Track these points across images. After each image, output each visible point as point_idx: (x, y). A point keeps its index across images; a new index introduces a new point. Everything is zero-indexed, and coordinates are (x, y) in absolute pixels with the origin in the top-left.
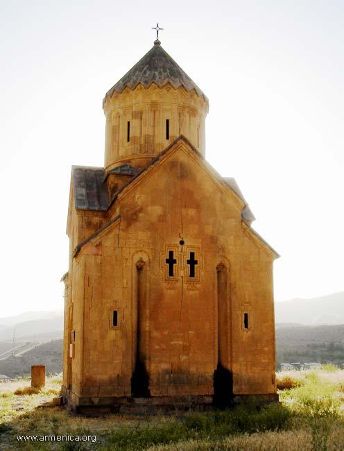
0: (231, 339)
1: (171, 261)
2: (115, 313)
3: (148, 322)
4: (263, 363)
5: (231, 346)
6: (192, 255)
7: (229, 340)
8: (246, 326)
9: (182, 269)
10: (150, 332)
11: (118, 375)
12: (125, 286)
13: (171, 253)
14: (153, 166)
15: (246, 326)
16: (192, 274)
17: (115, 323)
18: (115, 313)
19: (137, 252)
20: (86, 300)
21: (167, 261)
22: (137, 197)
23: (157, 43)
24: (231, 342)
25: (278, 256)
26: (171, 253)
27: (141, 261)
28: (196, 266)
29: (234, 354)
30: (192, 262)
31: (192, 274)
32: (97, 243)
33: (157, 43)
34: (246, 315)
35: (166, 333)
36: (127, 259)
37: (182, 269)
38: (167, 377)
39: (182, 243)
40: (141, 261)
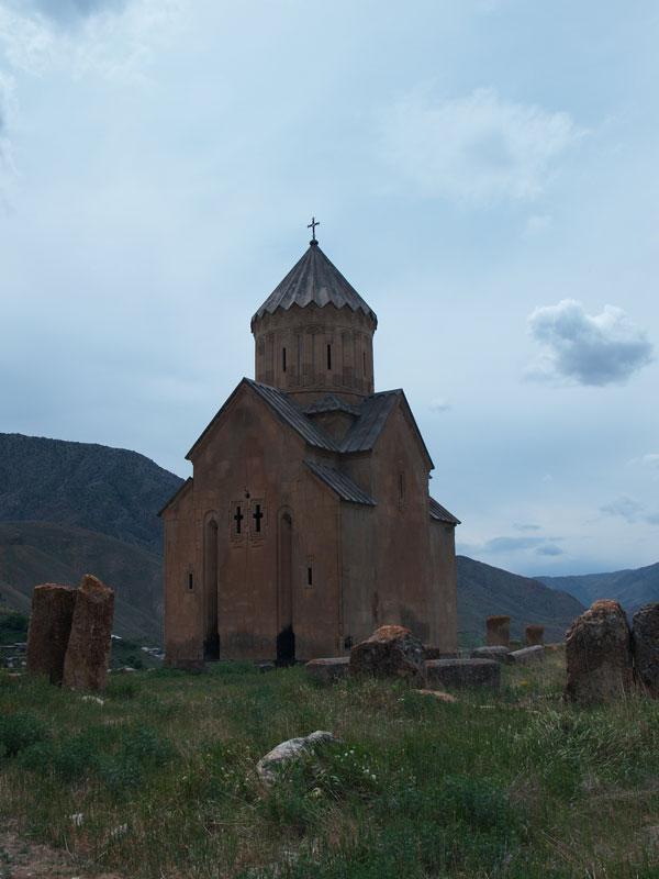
1: (239, 517)
6: (258, 507)
8: (310, 583)
9: (248, 522)
19: (209, 512)
23: (314, 243)
27: (213, 521)
30: (258, 516)
33: (314, 243)
34: (310, 570)
37: (248, 522)
39: (248, 496)
40: (213, 521)
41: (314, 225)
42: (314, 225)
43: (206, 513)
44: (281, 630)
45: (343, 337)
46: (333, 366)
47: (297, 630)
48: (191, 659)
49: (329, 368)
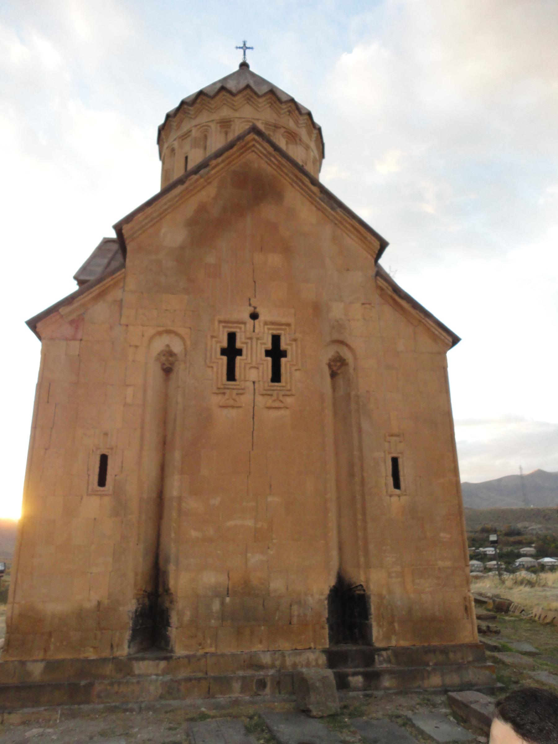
0: (364, 514)
2: (104, 459)
3: (177, 477)
4: (439, 569)
5: (365, 529)
6: (276, 339)
7: (360, 516)
8: (397, 485)
10: (180, 499)
11: (99, 603)
12: (129, 400)
13: (232, 337)
15: (397, 485)
16: (276, 377)
17: (102, 482)
18: (104, 459)
21: (224, 352)
22: (163, 231)
23: (244, 65)
24: (364, 521)
25: (455, 340)
26: (232, 337)
27: (169, 353)
28: (283, 360)
29: (371, 546)
31: (276, 377)
32: (74, 316)
33: (244, 65)
34: (395, 461)
35: (216, 501)
36: (136, 347)
38: (216, 606)
39: (254, 316)
40: (169, 353)
42: (245, 48)
44: (332, 582)
48: (91, 655)
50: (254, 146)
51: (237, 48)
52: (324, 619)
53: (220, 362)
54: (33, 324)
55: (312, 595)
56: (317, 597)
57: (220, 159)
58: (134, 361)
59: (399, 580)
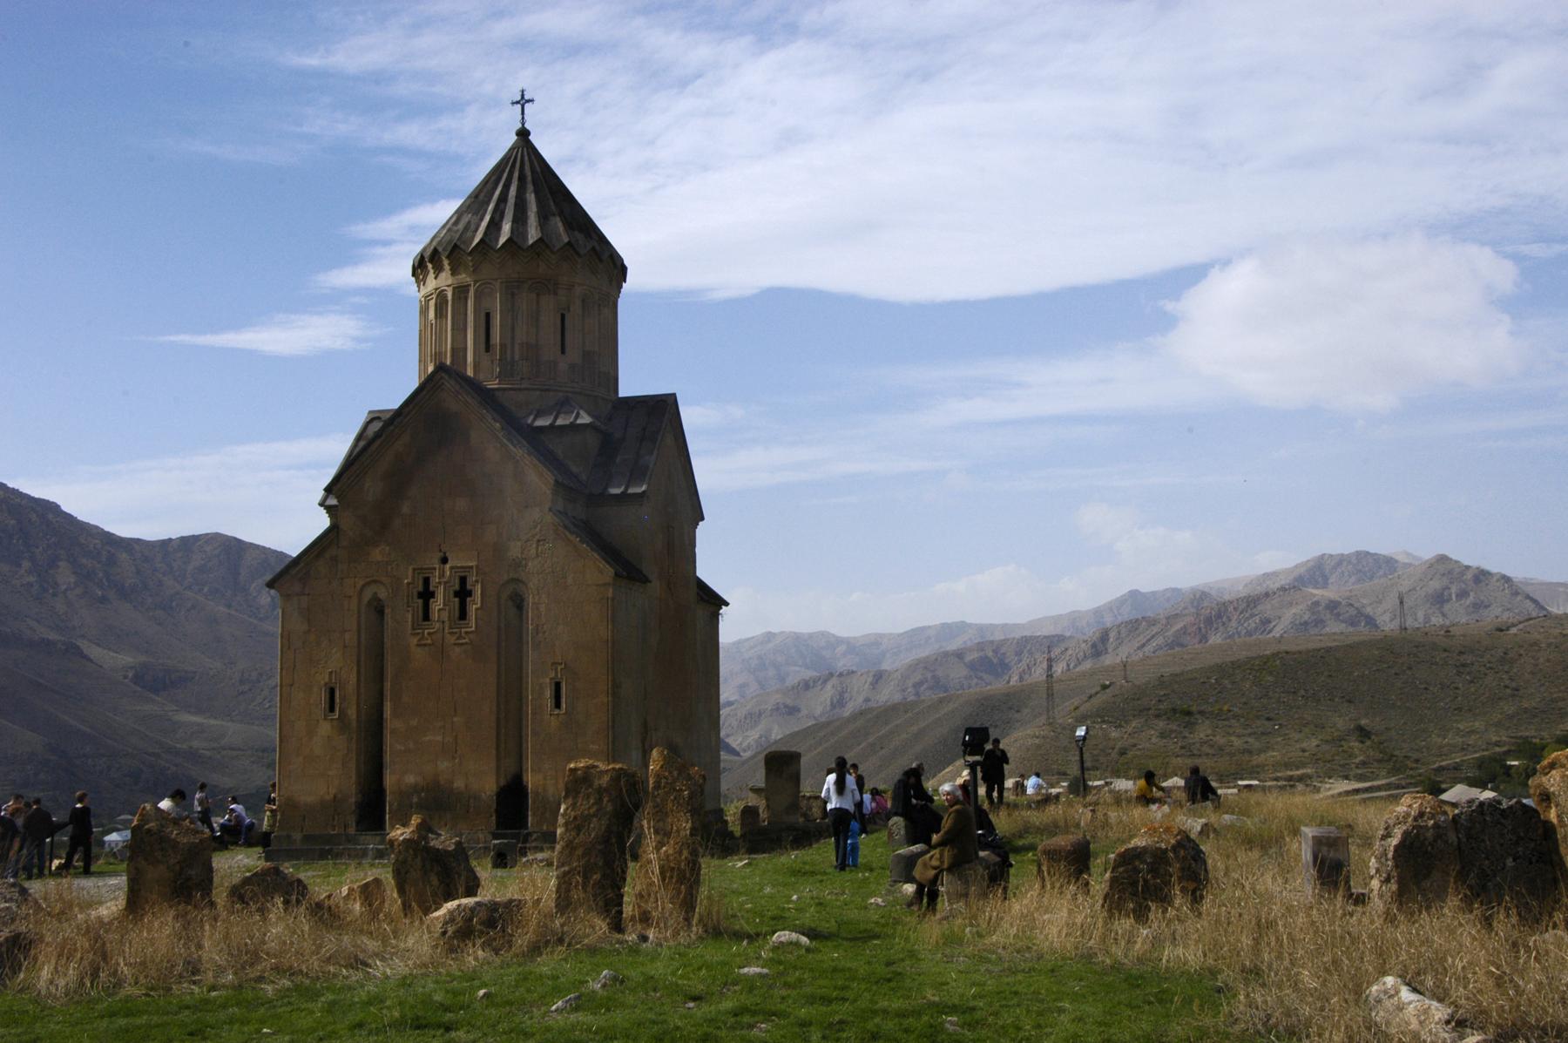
1: (427, 595)
2: (332, 692)
6: (463, 580)
11: (335, 797)
14: (392, 428)
18: (332, 692)
20: (284, 672)
21: (420, 595)
23: (523, 134)
33: (523, 134)
35: (414, 723)
36: (350, 597)
41: (523, 101)
42: (523, 101)
43: (364, 586)
44: (503, 782)
45: (583, 301)
46: (568, 350)
47: (531, 780)
49: (563, 352)
50: (443, 384)
51: (513, 103)
52: (493, 810)
53: (416, 605)
54: (270, 585)
55: (485, 793)
56: (488, 793)
57: (411, 406)
58: (349, 610)
59: (553, 781)
